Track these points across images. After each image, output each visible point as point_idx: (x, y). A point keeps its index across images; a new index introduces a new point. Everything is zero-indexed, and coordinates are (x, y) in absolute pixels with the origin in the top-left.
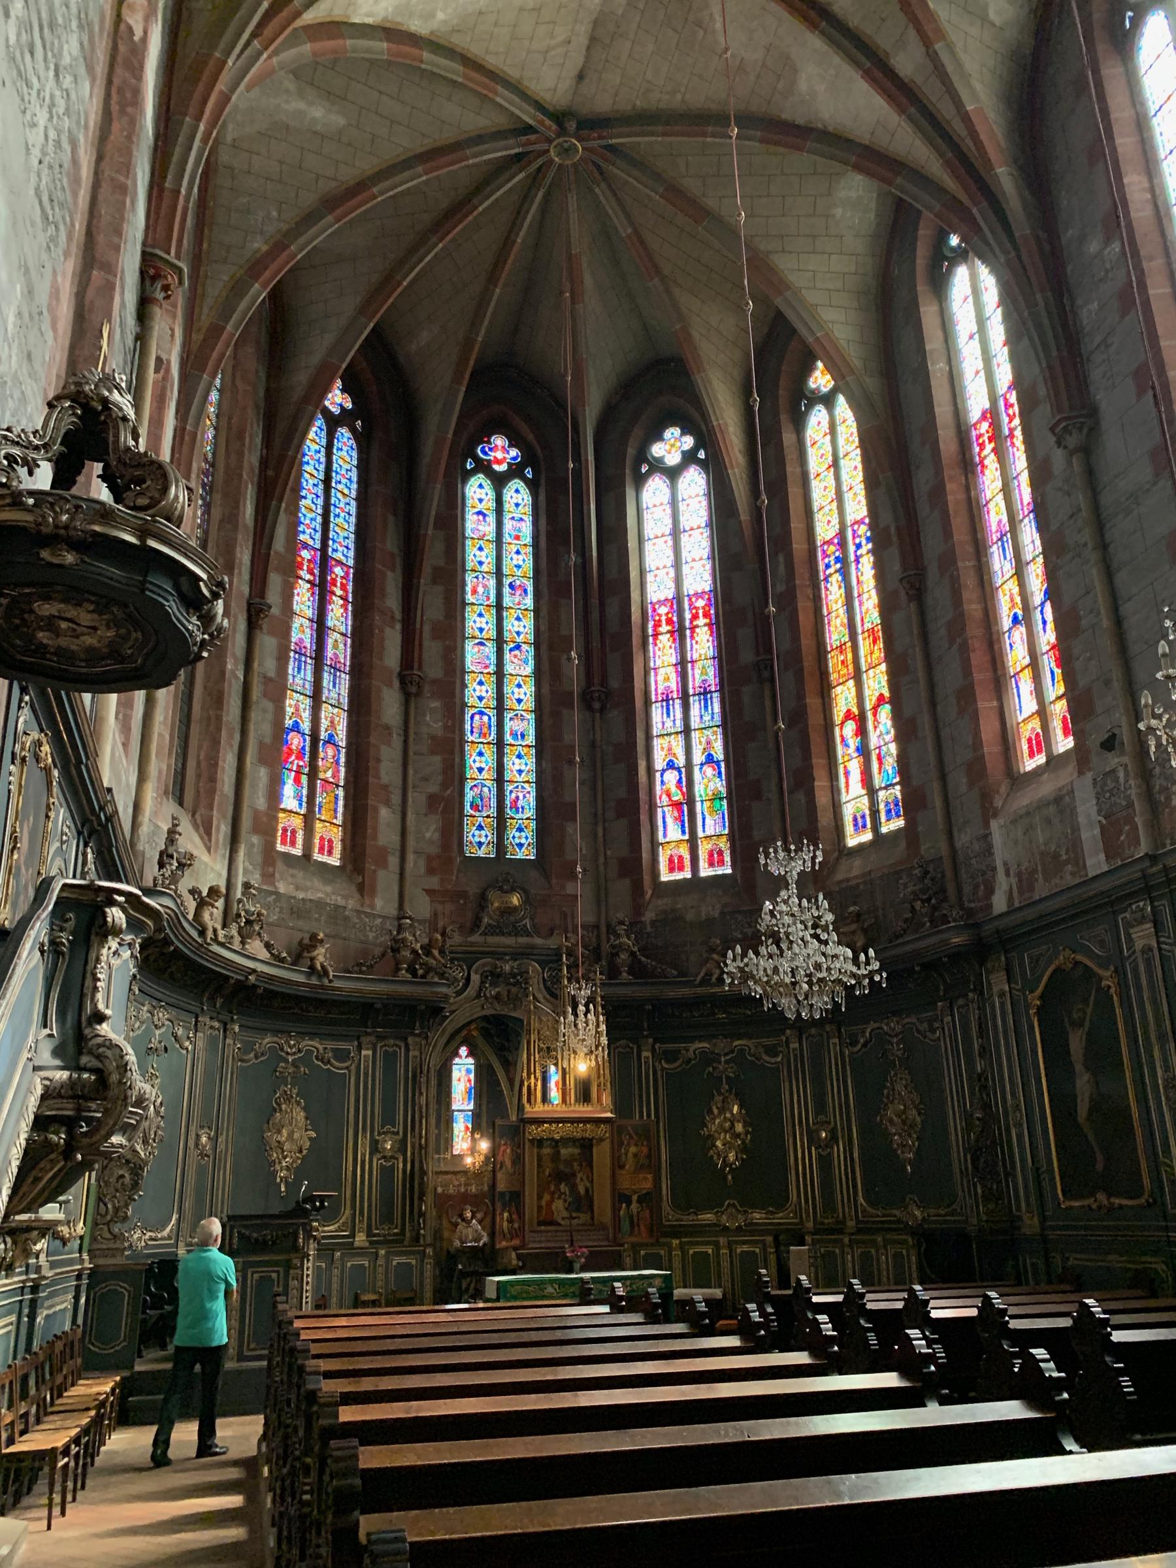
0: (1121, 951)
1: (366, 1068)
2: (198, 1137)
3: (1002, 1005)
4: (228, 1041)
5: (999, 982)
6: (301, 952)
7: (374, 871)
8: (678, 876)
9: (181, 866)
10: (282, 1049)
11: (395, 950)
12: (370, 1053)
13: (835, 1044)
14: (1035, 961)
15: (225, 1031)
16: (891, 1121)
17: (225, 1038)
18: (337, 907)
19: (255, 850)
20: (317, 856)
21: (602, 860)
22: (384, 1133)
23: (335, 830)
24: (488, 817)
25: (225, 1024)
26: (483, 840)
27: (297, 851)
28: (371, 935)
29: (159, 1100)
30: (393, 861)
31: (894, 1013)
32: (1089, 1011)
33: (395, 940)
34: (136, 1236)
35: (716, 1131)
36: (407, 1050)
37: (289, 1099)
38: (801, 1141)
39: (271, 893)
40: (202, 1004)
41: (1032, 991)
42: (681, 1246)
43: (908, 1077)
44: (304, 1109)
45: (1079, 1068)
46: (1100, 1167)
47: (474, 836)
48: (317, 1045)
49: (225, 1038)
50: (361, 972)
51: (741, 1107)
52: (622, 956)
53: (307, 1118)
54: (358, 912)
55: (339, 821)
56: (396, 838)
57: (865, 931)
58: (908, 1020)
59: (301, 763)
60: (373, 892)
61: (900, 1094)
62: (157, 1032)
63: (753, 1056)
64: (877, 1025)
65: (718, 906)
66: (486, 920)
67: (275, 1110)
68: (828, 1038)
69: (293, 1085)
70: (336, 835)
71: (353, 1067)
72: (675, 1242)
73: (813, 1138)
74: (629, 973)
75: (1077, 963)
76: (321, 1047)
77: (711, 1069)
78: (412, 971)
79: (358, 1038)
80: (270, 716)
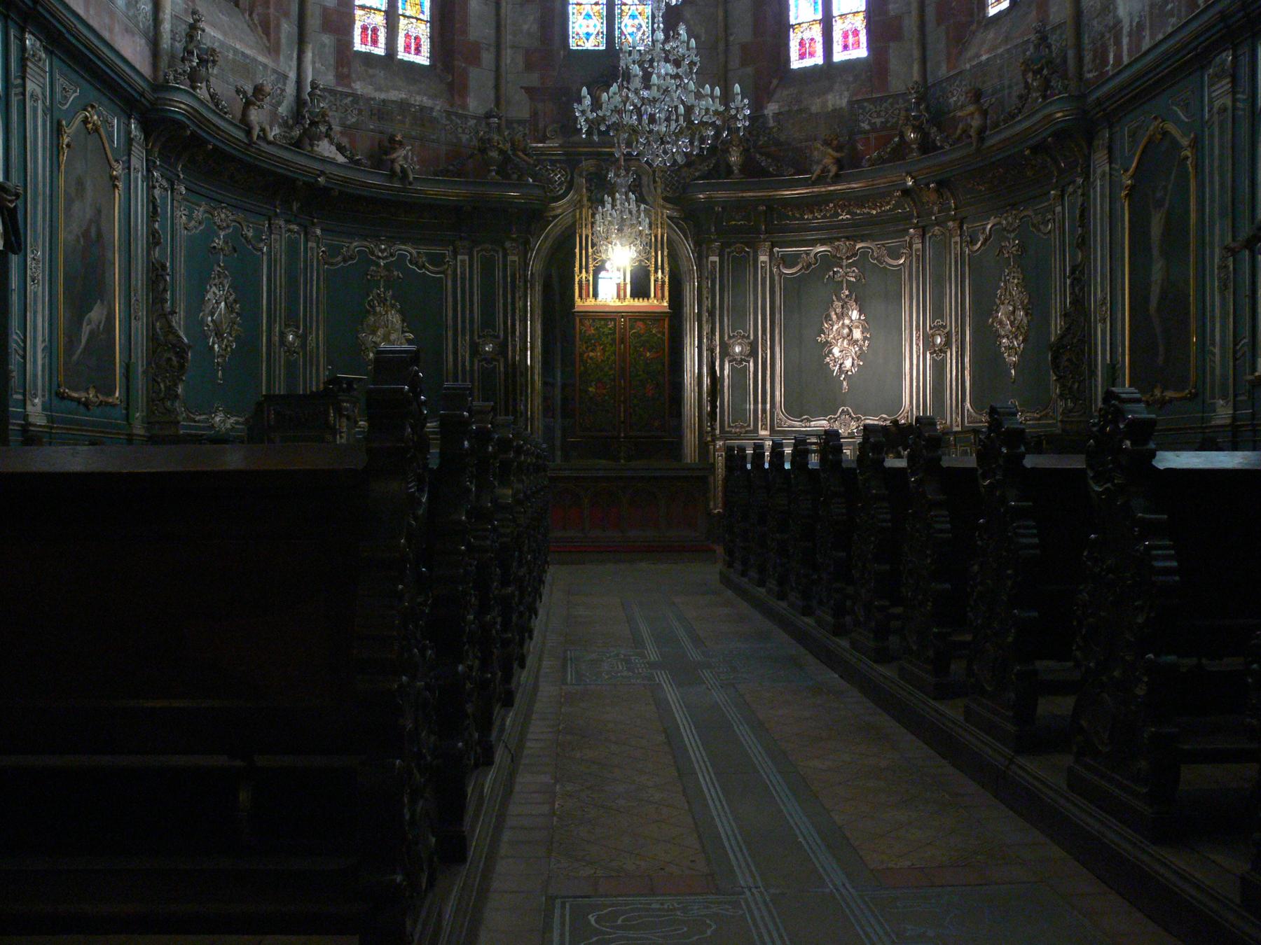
0: (1203, 116)
1: (463, 273)
2: (283, 335)
3: (1102, 186)
4: (310, 244)
5: (1100, 161)
6: (381, 155)
8: (808, 62)
9: (202, 62)
10: (372, 253)
11: (483, 151)
12: (466, 258)
13: (956, 243)
14: (1133, 135)
15: (306, 234)
16: (1001, 323)
17: (307, 241)
18: (422, 108)
19: (327, 50)
20: (402, 55)
21: (721, 46)
22: (484, 336)
24: (597, 4)
25: (306, 227)
26: (591, 30)
27: (380, 50)
28: (464, 138)
29: (231, 298)
30: (487, 57)
31: (1013, 206)
32: (1170, 187)
33: (481, 140)
34: (217, 419)
35: (834, 338)
36: (505, 256)
37: (383, 301)
38: (918, 346)
39: (347, 95)
40: (275, 207)
41: (1126, 170)
43: (1021, 277)
45: (1156, 253)
46: (1160, 360)
47: (581, 26)
48: (410, 249)
49: (307, 241)
51: (861, 312)
53: (403, 321)
54: (449, 114)
55: (426, 16)
56: (489, 32)
57: (984, 113)
58: (1026, 213)
61: (1011, 294)
62: (222, 234)
63: (876, 259)
64: (998, 219)
65: (846, 94)
67: (368, 312)
68: (951, 236)
70: (423, 31)
71: (449, 272)
73: (928, 343)
75: (1165, 133)
76: (415, 254)
77: (831, 273)
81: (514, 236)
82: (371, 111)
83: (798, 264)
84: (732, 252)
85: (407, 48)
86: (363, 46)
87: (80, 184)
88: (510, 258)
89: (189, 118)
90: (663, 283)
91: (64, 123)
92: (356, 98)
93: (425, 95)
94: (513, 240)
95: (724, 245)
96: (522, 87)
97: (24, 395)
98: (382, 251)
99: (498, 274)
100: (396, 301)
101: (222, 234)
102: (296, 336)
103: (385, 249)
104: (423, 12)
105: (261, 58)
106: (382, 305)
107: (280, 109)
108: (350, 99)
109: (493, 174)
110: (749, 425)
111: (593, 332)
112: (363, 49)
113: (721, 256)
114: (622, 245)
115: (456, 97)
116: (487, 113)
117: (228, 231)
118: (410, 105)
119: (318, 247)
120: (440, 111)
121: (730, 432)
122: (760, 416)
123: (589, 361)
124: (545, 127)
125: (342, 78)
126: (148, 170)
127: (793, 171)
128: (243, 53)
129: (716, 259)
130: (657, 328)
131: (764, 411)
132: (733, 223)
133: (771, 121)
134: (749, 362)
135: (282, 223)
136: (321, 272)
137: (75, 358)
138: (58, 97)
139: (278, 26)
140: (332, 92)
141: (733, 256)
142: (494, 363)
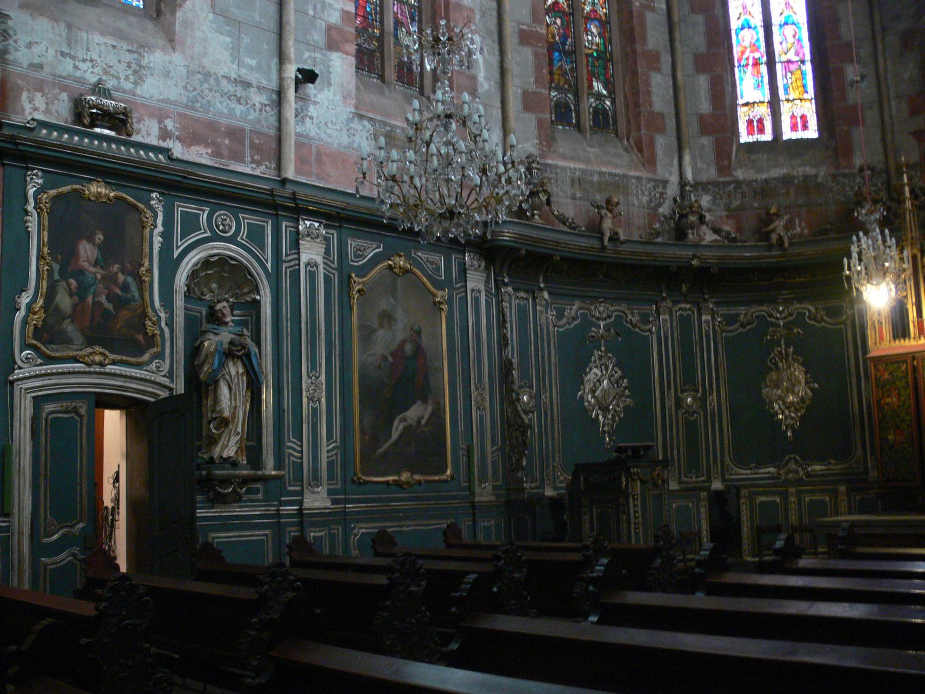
4: (704, 318)
10: (771, 316)
15: (699, 310)
18: (806, 178)
23: (808, 103)
27: (768, 136)
30: (871, 116)
39: (729, 183)
44: (803, 365)
49: (700, 316)
53: (806, 373)
59: (757, 55)
62: (602, 324)
67: (771, 369)
69: (787, 346)
80: (701, 28)
82: (754, 192)
85: (794, 128)
86: (750, 136)
87: (387, 318)
89: (516, 242)
91: (353, 275)
92: (738, 183)
96: (910, 133)
97: (302, 486)
98: (778, 312)
101: (602, 324)
102: (694, 398)
103: (783, 310)
104: (806, 92)
105: (632, 173)
106: (784, 361)
107: (661, 210)
108: (732, 186)
112: (751, 139)
117: (609, 321)
118: (794, 177)
119: (713, 318)
120: (825, 175)
123: (886, 407)
125: (723, 169)
126: (498, 288)
128: (610, 174)
135: (669, 303)
136: (719, 339)
137: (381, 450)
138: (351, 256)
139: (652, 144)
140: (716, 184)
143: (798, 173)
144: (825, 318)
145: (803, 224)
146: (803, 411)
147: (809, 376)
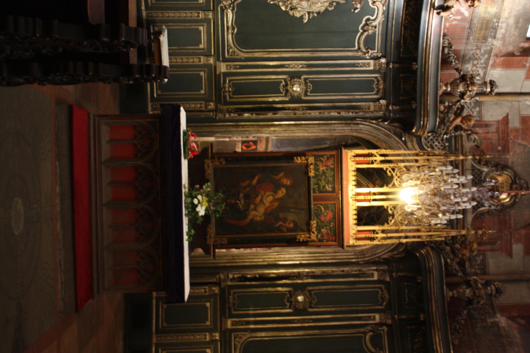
7: (524, 66)
12: (372, 68)
18: (495, 29)
22: (306, 83)
33: (472, 77)
42: (213, 341)
44: (326, 10)
50: (444, 48)
52: (468, 291)
53: (318, 13)
60: (507, 65)
66: (485, 169)
71: (360, 54)
72: (217, 336)
74: (452, 297)
78: (445, 93)
79: (384, 56)
81: (390, 108)
83: (374, 347)
84: (382, 291)
88: (372, 104)
90: (372, 239)
93: (506, 32)
94: (387, 106)
95: (387, 284)
96: (508, 114)
99: (358, 95)
100: (335, 7)
109: (444, 88)
110: (235, 310)
111: (321, 169)
113: (378, 281)
114: (420, 195)
115: (502, 58)
116: (494, 81)
120: (492, 45)
121: (229, 294)
122: (243, 319)
124: (476, 133)
127: (456, 342)
129: (376, 278)
130: (327, 234)
131: (248, 323)
132: (406, 291)
133: (491, 320)
134: (290, 308)
141: (378, 292)
142: (284, 92)
143: (502, 22)
144: (366, 34)
145: (454, 23)
146: (283, 8)
147: (316, 15)
